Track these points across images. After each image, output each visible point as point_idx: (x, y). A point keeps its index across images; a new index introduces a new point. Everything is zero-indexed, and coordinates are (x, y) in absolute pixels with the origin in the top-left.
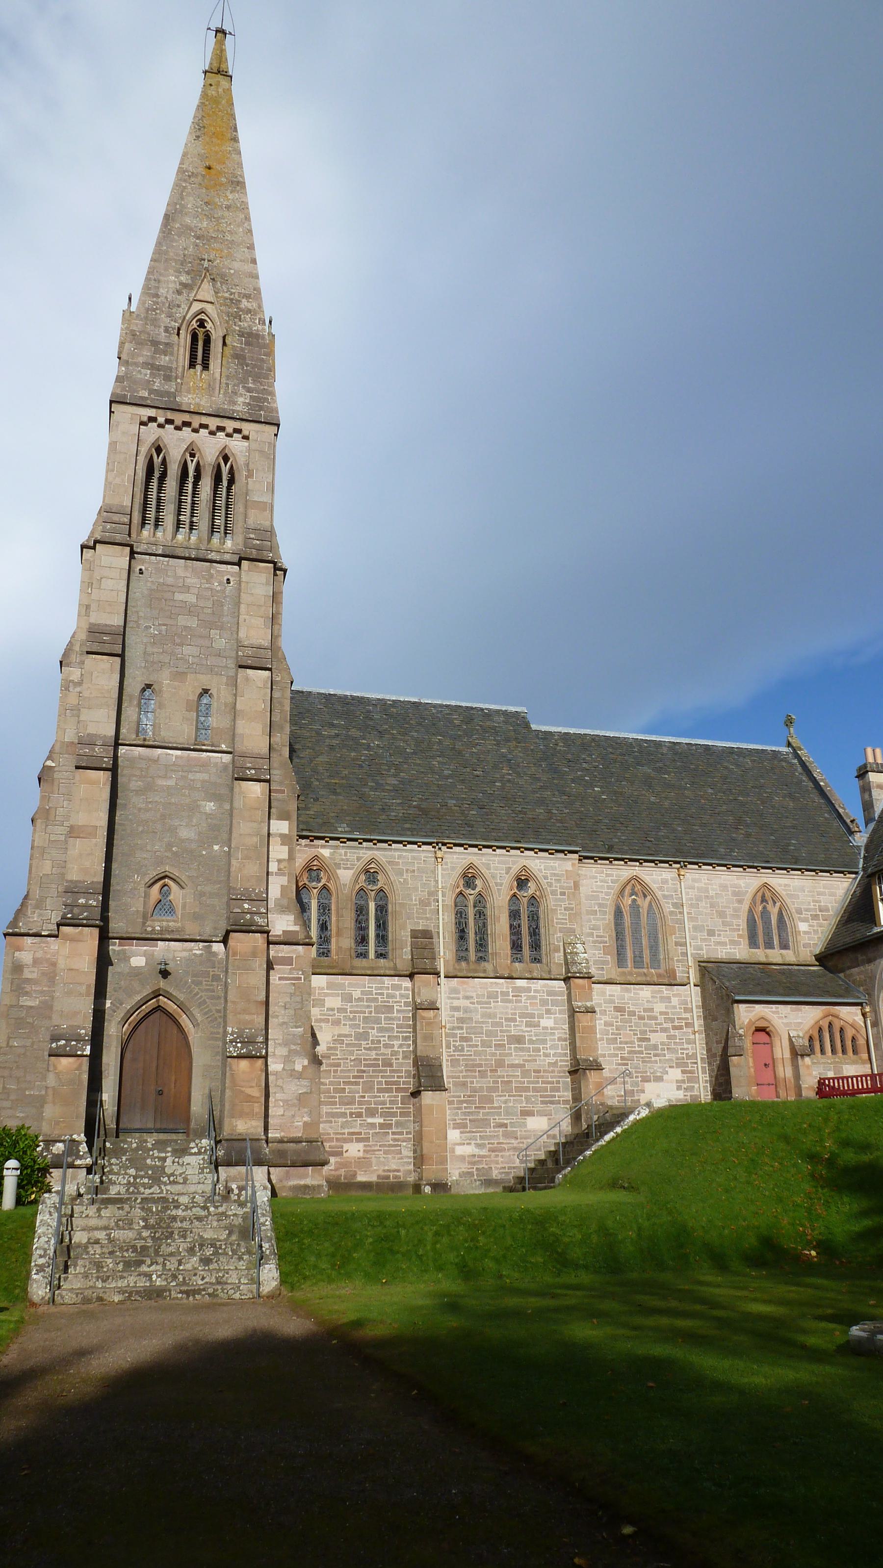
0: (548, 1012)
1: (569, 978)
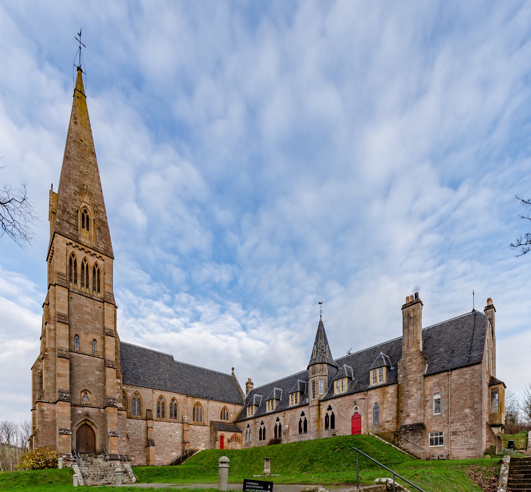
0: (178, 430)
1: (183, 423)
